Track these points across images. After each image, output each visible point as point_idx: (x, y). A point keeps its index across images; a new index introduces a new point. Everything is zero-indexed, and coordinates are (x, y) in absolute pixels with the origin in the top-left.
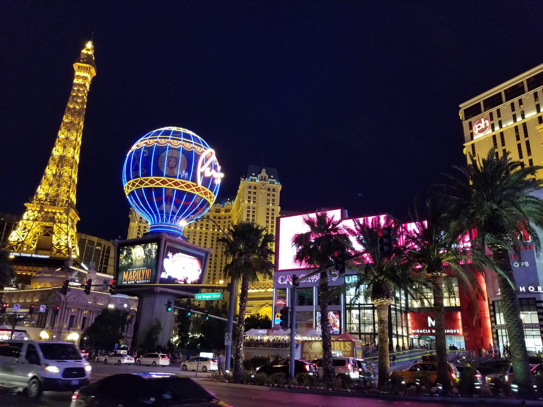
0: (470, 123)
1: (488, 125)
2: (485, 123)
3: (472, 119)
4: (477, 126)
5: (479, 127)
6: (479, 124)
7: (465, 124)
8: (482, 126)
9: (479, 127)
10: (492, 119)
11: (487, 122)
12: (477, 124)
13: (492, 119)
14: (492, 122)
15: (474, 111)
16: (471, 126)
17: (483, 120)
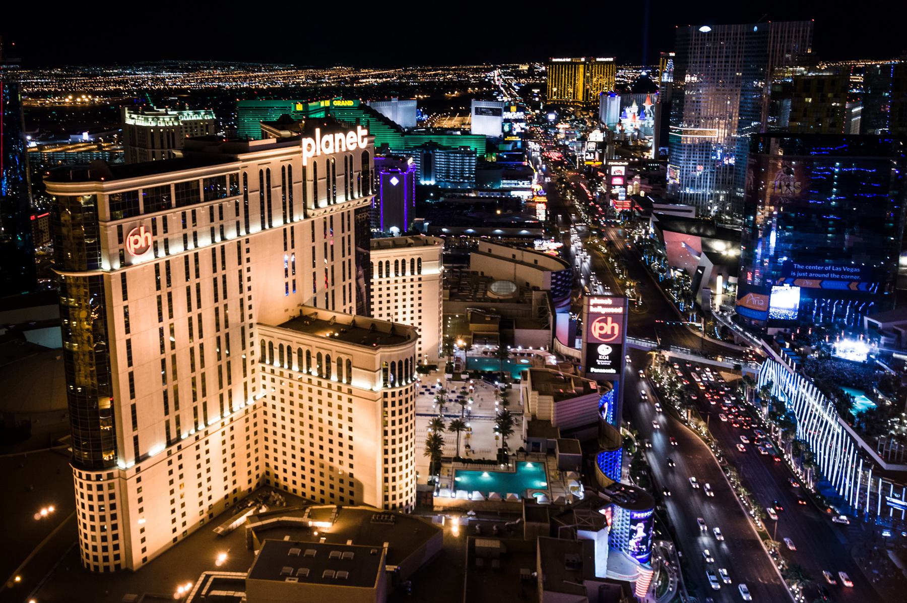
0: (120, 227)
1: (150, 243)
3: (126, 223)
4: (132, 239)
5: (136, 242)
6: (137, 237)
8: (141, 242)
9: (136, 242)
10: (155, 234)
12: (133, 235)
13: (155, 234)
14: (155, 238)
17: (142, 229)
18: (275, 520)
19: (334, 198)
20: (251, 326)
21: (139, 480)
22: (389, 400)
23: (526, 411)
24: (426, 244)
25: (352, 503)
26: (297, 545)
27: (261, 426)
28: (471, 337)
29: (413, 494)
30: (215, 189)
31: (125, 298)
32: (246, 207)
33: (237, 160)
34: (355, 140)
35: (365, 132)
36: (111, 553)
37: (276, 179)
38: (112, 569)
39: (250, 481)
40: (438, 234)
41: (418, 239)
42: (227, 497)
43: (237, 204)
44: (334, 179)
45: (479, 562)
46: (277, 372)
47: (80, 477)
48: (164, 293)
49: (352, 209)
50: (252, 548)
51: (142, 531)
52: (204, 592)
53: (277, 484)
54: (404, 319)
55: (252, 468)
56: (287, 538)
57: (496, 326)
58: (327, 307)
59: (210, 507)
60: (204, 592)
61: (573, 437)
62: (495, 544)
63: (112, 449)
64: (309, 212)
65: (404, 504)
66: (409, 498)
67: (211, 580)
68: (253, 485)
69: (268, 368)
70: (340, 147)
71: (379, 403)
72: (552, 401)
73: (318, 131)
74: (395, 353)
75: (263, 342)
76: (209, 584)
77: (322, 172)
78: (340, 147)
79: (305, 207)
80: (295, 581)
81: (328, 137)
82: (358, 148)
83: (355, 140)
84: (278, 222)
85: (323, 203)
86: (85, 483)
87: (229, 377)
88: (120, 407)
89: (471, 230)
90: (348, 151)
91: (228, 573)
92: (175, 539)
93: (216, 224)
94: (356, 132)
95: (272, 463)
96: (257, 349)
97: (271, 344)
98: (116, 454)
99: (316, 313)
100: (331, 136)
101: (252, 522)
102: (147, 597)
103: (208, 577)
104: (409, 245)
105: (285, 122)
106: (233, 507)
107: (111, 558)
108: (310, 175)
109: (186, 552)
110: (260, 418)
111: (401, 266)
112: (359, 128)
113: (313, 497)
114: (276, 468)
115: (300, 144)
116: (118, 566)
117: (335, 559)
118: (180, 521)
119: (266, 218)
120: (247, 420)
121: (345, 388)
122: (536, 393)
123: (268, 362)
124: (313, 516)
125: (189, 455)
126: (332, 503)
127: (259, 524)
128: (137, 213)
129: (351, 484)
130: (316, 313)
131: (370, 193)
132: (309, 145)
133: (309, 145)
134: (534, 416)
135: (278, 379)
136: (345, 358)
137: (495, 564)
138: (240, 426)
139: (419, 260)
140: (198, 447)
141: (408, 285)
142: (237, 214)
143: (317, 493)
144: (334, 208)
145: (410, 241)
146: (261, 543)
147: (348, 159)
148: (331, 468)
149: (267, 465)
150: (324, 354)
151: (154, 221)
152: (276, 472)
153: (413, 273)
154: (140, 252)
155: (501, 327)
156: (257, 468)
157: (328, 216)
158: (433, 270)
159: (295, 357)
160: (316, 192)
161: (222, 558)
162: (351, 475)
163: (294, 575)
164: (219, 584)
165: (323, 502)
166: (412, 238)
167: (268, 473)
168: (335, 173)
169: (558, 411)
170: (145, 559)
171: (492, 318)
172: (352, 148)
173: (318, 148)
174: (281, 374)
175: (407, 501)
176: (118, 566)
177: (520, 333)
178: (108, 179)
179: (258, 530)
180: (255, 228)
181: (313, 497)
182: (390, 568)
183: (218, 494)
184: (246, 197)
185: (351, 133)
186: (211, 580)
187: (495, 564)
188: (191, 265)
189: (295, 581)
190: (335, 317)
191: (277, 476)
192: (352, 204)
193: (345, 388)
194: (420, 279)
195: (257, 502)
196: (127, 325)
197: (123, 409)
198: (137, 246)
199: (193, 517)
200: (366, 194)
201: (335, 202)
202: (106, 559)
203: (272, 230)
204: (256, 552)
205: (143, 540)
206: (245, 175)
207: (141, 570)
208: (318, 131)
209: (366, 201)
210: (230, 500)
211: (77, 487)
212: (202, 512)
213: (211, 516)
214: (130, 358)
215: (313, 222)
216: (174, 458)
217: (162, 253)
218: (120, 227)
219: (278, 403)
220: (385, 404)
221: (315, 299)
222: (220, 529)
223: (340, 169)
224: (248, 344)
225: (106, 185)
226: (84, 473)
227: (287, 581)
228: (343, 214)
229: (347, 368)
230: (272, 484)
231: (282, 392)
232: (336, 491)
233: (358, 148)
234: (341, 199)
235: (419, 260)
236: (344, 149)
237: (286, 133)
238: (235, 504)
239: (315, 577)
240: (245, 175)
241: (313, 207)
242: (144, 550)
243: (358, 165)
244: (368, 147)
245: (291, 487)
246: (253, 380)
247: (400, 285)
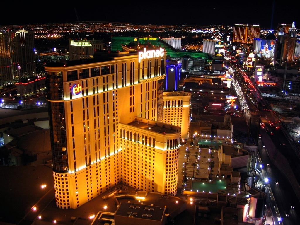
0: (70, 84)
1: (81, 90)
2: (79, 88)
3: (73, 82)
5: (76, 90)
6: (76, 88)
8: (78, 90)
9: (76, 90)
12: (75, 87)
13: (83, 87)
14: (83, 88)
17: (78, 85)
18: (125, 195)
19: (150, 75)
20: (117, 123)
21: (76, 178)
22: (169, 154)
23: (220, 160)
24: (184, 95)
25: (153, 191)
26: (133, 204)
27: (120, 161)
28: (200, 132)
29: (176, 189)
30: (106, 71)
32: (117, 78)
33: (113, 60)
34: (159, 53)
35: (163, 50)
36: (66, 202)
37: (128, 67)
38: (67, 208)
39: (115, 181)
40: (189, 91)
41: (182, 93)
42: (107, 186)
43: (113, 76)
44: (150, 68)
45: (199, 215)
46: (126, 141)
47: (56, 175)
49: (157, 80)
50: (116, 205)
51: (77, 195)
52: (99, 218)
53: (125, 183)
54: (174, 123)
55: (116, 176)
56: (129, 202)
57: (210, 128)
58: (146, 118)
59: (101, 189)
60: (99, 218)
61: (238, 171)
62: (206, 208)
63: (67, 166)
64: (140, 81)
65: (173, 192)
66: (174, 190)
67: (102, 214)
68: (116, 182)
69: (123, 140)
70: (153, 56)
71: (165, 155)
72: (230, 157)
73: (145, 49)
74: (172, 136)
75: (121, 130)
76: (101, 215)
77: (146, 65)
78: (153, 56)
79: (139, 79)
80: (132, 217)
81: (149, 52)
82: (160, 56)
83: (159, 53)
84: (128, 84)
85: (146, 77)
86: (57, 177)
87: (109, 143)
88: (69, 151)
89: (201, 90)
90: (156, 57)
91: (109, 213)
92: (88, 200)
93: (106, 84)
94: (159, 49)
95: (124, 175)
96: (119, 132)
97: (124, 131)
98: (68, 168)
99: (142, 120)
100: (150, 51)
101: (116, 196)
102: (79, 218)
103: (100, 213)
104: (178, 95)
105: (132, 45)
106: (109, 190)
107: (67, 204)
108: (141, 66)
109: (93, 203)
110: (120, 158)
111: (174, 103)
112: (161, 48)
113: (139, 188)
114: (125, 177)
115: (137, 54)
116: (69, 207)
117: (147, 210)
118: (90, 193)
119: (124, 82)
120: (115, 159)
121: (152, 149)
122: (224, 154)
123: (123, 137)
124: (139, 195)
125: (94, 170)
126: (145, 191)
127: (119, 196)
128: (77, 79)
129: (153, 184)
130: (142, 120)
131: (164, 74)
132: (141, 55)
133: (141, 55)
134: (223, 163)
135: (126, 144)
136: (152, 137)
137: (205, 215)
138: (112, 161)
139: (182, 101)
140: (97, 168)
141: (177, 111)
143: (140, 188)
144: (150, 79)
145: (178, 93)
146: (120, 203)
147: (156, 60)
148: (146, 178)
149: (122, 176)
150: (145, 135)
151: (83, 82)
152: (125, 178)
153: (179, 106)
154: (77, 93)
155: (212, 128)
156: (118, 176)
157: (147, 83)
158: (186, 106)
159: (133, 136)
160: (143, 73)
161: (105, 207)
162: (153, 181)
163: (132, 215)
164: (104, 216)
165: (142, 190)
166: (179, 92)
167: (122, 179)
168: (151, 66)
169: (233, 161)
170: (78, 206)
171: (208, 125)
172: (158, 56)
173: (145, 55)
174: (128, 142)
175: (174, 192)
176: (69, 207)
177: (218, 131)
178: (67, 66)
179: (119, 199)
180: (120, 86)
181: (139, 188)
182: (167, 215)
183: (104, 185)
184: (117, 74)
185: (158, 50)
186: (102, 214)
187: (205, 215)
188: (96, 99)
189: (132, 217)
190: (149, 122)
191: (125, 180)
192: (157, 78)
193: (152, 149)
194: (182, 109)
195: (118, 188)
197: (71, 152)
198: (76, 91)
199: (95, 192)
200: (162, 74)
201: (150, 77)
202: (65, 204)
204: (118, 206)
205: (77, 199)
206: (117, 66)
207: (76, 209)
208: (145, 49)
209: (162, 77)
210: (108, 188)
211: (55, 178)
212: (98, 191)
213: (101, 192)
215: (142, 85)
216: (88, 171)
217: (85, 95)
218: (70, 84)
219: (126, 153)
220: (167, 156)
221: (141, 114)
222: (104, 197)
223: (153, 64)
224: (116, 130)
225: (66, 68)
226: (57, 174)
227: (129, 216)
228: (153, 82)
229: (153, 142)
230: (123, 183)
231: (128, 149)
232: (147, 187)
233: (160, 56)
234: (153, 76)
235: (182, 101)
236: (154, 57)
237: (132, 50)
238: (109, 189)
239: (139, 216)
240: (117, 66)
241: (142, 79)
242: (78, 202)
243: (159, 63)
244: (164, 56)
245: (130, 184)
246: (117, 144)
247: (174, 111)
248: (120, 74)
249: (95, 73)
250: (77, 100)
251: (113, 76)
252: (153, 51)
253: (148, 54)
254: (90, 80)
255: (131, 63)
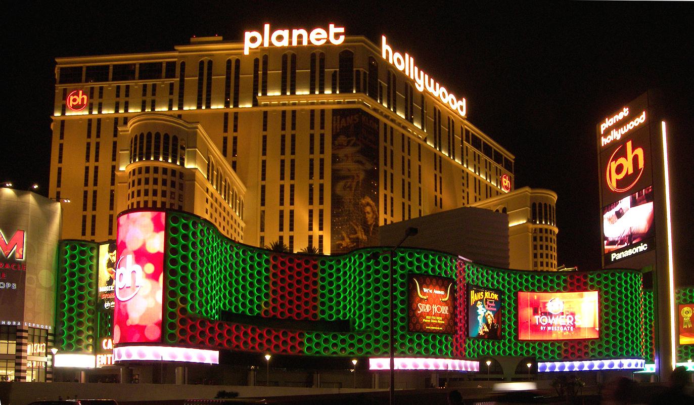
2: (81, 98)
5: (74, 100)
6: (75, 97)
7: (59, 88)
9: (74, 100)
11: (85, 97)
12: (73, 95)
14: (91, 101)
15: (72, 76)
16: (65, 97)
17: (81, 92)
30: (150, 71)
31: (62, 137)
48: (93, 140)
84: (218, 106)
119: (203, 99)
142: (171, 93)
154: (77, 107)
184: (182, 81)
196: (60, 157)
198: (75, 103)
203: (208, 111)
206: (183, 64)
208: (267, 27)
214: (59, 182)
240: (183, 64)
248: (192, 80)
249: (123, 72)
250: (77, 121)
251: (172, 85)
252: (303, 32)
253: (280, 38)
254: (110, 86)
255: (229, 62)
